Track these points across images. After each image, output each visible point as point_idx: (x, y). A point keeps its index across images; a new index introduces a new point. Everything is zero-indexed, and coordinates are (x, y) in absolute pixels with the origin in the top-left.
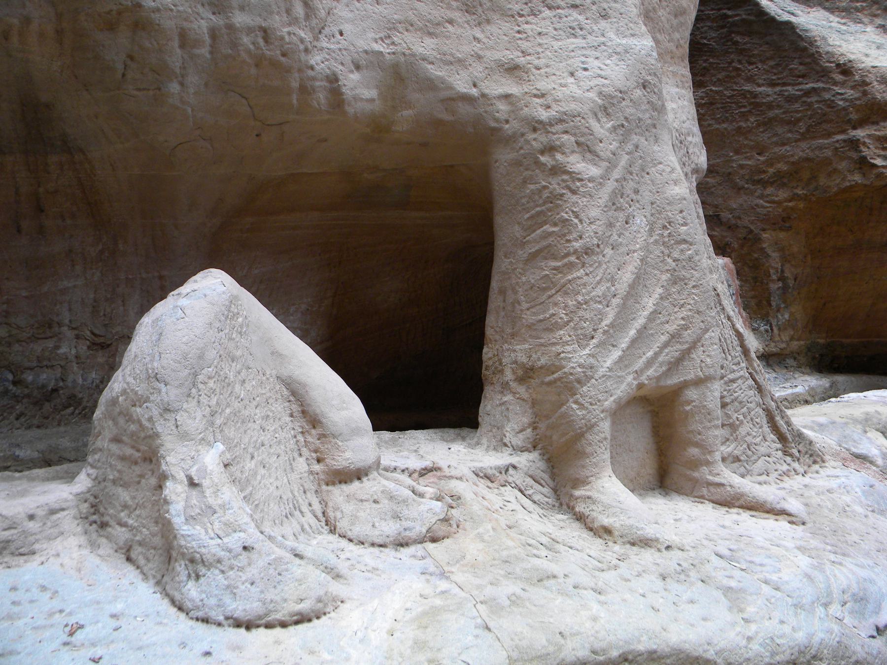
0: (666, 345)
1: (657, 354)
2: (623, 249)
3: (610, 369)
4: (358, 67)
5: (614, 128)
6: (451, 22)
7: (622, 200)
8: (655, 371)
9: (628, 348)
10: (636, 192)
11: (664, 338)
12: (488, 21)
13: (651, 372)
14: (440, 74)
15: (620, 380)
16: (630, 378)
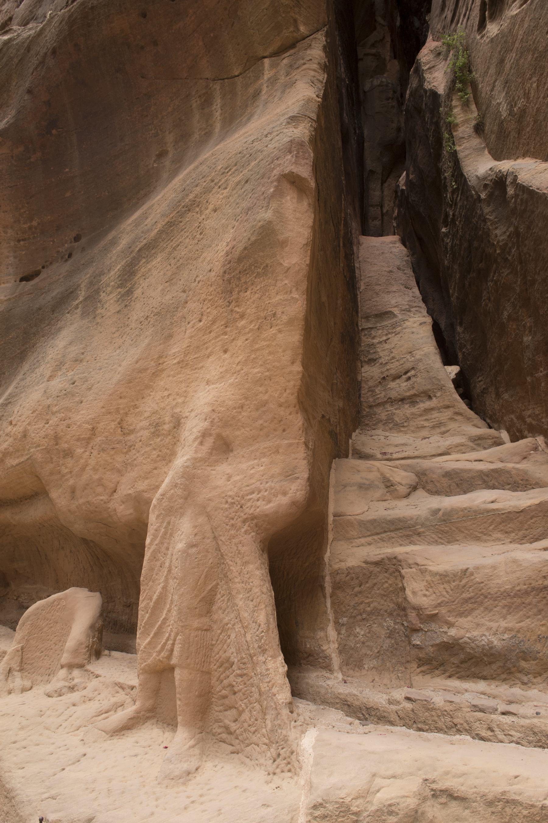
0: (168, 639)
1: (165, 644)
2: (157, 582)
3: (145, 648)
4: (123, 503)
5: (158, 516)
6: (155, 469)
7: (159, 555)
8: (164, 654)
9: (153, 637)
10: (168, 549)
11: (167, 635)
12: (170, 461)
13: (162, 654)
14: (149, 496)
15: (150, 654)
16: (154, 655)
